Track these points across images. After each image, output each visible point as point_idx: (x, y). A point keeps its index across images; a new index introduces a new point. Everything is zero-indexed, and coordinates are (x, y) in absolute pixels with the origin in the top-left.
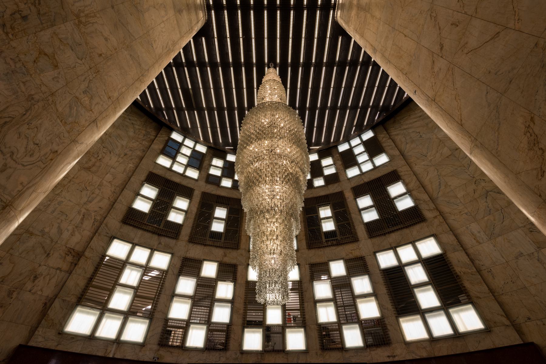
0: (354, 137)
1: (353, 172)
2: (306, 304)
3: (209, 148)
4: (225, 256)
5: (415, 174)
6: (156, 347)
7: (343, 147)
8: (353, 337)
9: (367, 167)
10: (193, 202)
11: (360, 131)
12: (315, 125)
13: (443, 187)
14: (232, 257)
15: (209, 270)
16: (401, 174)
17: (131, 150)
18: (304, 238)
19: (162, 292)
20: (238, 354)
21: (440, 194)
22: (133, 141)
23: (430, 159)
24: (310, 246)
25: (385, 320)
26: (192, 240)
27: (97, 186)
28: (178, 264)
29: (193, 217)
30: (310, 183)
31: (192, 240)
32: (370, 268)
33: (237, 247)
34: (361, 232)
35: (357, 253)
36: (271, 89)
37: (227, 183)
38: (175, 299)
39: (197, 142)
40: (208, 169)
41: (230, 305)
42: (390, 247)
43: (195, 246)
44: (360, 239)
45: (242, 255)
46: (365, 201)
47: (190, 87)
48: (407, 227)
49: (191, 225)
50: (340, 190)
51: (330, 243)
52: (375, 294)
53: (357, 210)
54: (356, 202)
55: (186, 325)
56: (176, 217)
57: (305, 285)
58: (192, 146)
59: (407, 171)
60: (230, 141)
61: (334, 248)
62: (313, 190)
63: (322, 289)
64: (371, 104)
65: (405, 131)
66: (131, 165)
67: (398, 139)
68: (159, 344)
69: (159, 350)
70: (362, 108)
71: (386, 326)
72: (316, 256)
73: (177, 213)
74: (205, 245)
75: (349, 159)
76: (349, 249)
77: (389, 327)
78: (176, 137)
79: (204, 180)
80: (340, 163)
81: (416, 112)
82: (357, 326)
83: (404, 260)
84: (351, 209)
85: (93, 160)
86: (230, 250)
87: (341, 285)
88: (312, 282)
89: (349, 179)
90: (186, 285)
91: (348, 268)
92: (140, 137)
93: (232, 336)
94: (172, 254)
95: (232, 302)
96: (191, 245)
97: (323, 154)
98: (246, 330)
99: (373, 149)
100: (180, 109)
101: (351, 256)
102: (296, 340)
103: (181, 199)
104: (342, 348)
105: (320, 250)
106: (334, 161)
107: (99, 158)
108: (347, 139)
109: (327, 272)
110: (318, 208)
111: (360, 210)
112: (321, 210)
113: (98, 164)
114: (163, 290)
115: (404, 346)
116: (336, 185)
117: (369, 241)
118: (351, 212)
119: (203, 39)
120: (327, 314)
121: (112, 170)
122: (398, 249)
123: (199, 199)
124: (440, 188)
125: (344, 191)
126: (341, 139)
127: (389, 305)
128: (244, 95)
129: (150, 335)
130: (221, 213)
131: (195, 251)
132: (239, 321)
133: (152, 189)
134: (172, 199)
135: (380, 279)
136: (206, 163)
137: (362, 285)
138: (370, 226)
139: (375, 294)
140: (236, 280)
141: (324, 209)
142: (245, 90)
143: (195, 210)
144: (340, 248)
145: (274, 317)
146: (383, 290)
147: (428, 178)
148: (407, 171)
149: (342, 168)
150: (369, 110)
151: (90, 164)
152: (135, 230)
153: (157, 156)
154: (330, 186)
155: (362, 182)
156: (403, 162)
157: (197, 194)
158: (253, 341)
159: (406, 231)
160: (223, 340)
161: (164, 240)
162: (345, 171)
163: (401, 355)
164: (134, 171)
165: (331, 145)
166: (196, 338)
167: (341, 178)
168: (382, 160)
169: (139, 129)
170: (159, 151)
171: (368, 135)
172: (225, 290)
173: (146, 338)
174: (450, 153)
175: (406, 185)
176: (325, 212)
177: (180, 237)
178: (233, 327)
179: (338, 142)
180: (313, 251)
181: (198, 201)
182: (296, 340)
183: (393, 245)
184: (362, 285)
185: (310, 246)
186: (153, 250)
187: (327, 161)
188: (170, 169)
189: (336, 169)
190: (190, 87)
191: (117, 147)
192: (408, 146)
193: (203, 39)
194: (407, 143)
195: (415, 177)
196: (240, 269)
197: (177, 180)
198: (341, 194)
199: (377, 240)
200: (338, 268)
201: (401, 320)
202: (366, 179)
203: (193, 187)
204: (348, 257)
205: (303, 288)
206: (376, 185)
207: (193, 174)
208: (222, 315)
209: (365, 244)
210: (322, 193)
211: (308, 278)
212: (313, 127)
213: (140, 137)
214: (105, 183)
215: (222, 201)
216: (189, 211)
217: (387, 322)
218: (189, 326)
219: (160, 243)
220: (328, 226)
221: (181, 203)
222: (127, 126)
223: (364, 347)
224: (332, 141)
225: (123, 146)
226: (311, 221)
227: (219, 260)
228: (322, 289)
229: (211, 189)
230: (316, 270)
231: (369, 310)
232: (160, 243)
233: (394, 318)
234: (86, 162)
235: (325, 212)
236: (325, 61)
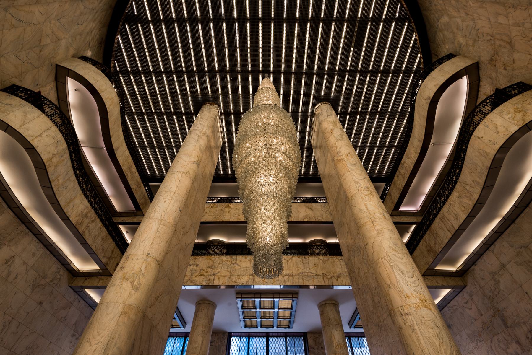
13: (14, 22)
21: (9, 16)
22: (449, 13)
23: (53, 22)
27: (521, 28)
36: (267, 93)
65: (95, 11)
66: (471, 4)
81: (98, 30)
85: (498, 43)
107: (492, 38)
113: (498, 37)
121: (492, 19)
124: (16, 19)
142: (295, 46)
147: (37, 13)
151: (503, 44)
174: (42, 44)
191: (468, 26)
192: (83, 7)
194: (85, 8)
213: (440, 9)
214: (511, 22)
225: (463, 21)
234: (505, 48)
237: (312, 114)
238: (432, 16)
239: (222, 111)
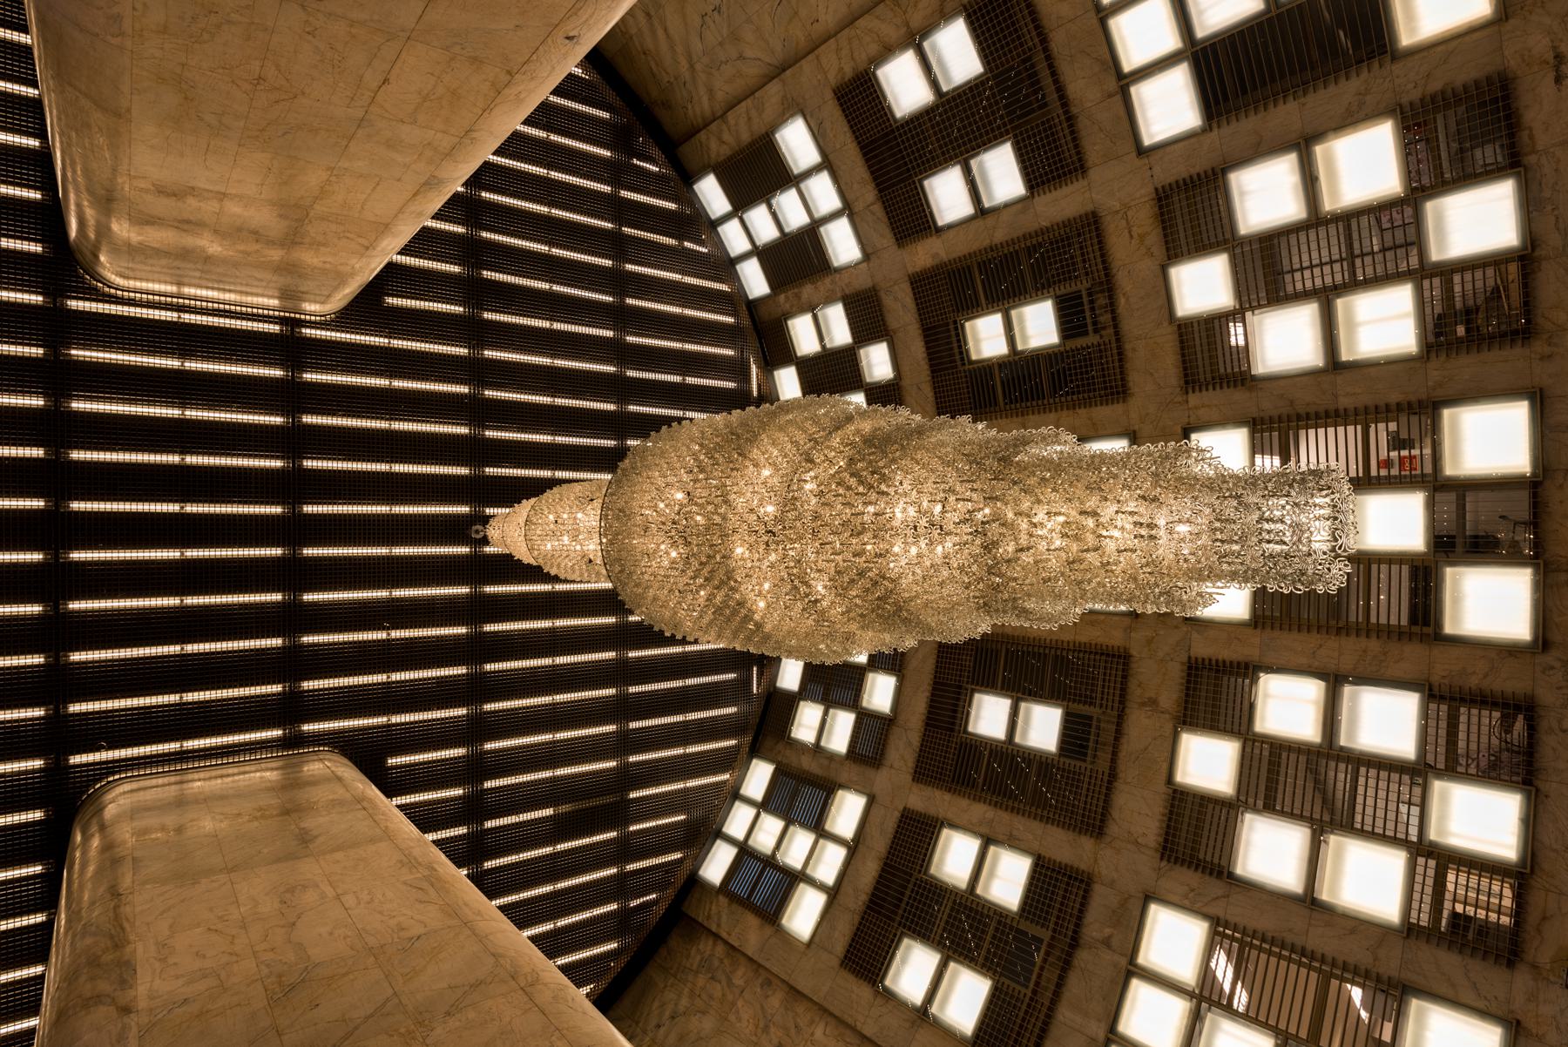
0: (719, 244)
1: (842, 244)
2: (1345, 402)
3: (755, 751)
4: (1153, 702)
5: (851, 21)
6: (1522, 979)
7: (754, 280)
8: (1478, 221)
9: (824, 193)
10: (950, 815)
11: (697, 223)
12: (677, 379)
14: (1158, 679)
15: (1208, 763)
16: (849, 72)
17: (766, 1029)
18: (1082, 412)
19: (1299, 941)
20: (1549, 658)
22: (732, 1018)
24: (1117, 390)
25: (1405, 100)
26: (1094, 822)
28: (1188, 877)
29: (1005, 816)
30: (882, 395)
31: (1094, 822)
32: (1200, 165)
33: (1120, 660)
34: (1064, 203)
35: (1144, 217)
36: (556, 532)
37: (880, 692)
38: (1324, 895)
40: (832, 756)
41: (1347, 690)
42: (1118, 98)
43: (1115, 813)
44: (1090, 208)
45: (1150, 641)
46: (947, 195)
47: (549, 812)
48: (1044, 40)
49: (1037, 826)
50: (906, 287)
51: (1105, 318)
52: (1303, 145)
53: (980, 223)
54: (950, 227)
55: (1433, 860)
56: (1008, 883)
57: (1268, 405)
58: (752, 812)
59: (838, 50)
60: (732, 676)
61: (1122, 301)
62: (906, 383)
63: (1284, 341)
64: (607, 189)
65: (698, 67)
66: (819, 1033)
67: (724, 89)
68: (1511, 964)
69: (1535, 967)
70: (619, 220)
71: (1433, 97)
72: (1152, 367)
73: (992, 874)
74: (1113, 775)
75: (796, 259)
76: (1128, 249)
77: (1436, 86)
78: (717, 865)
79: (870, 772)
80: (807, 291)
81: (633, 31)
82: (1430, 207)
83: (1170, 41)
84: (976, 246)
86: (1133, 684)
87: (1267, 270)
88: (1254, 378)
89: (867, 256)
90: (1270, 851)
91: (1201, 248)
92: (718, 993)
93: (1473, 682)
94: (1148, 898)
95: (1335, 681)
96: (1113, 829)
97: (778, 351)
98: (1448, 629)
99: (758, 175)
100: (624, 850)
101: (1154, 238)
102: (1491, 439)
103: (942, 860)
104: (1523, 261)
105: (1129, 354)
106: (802, 310)
108: (726, 266)
109: (1214, 323)
110: (971, 362)
111: (981, 211)
112: (978, 351)
114: (1289, 938)
115: (1511, 21)
116: (887, 301)
117: (1093, 174)
118: (987, 243)
119: (392, 761)
120: (1384, 323)
122: (1128, 66)
123: (938, 793)
125: (911, 270)
126: (725, 288)
127: (1348, 89)
128: (576, 628)
129: (1469, 997)
130: (989, 716)
131: (1138, 814)
132: (1413, 656)
133: (904, 961)
134: (941, 890)
135: (1244, 127)
136: (808, 764)
137: (1265, 195)
138: (1036, 175)
139: (1303, 145)
140: (1247, 666)
141: (977, 341)
143: (980, 811)
144: (1123, 280)
145: (1395, 523)
146: (1286, 114)
148: (838, 50)
149: (827, 281)
150: (624, 193)
152: (1055, 1031)
153: (787, 938)
154: (892, 323)
155: (878, 209)
156: (807, 66)
157: (922, 799)
158: (1492, 603)
159: (1058, 41)
160: (1516, 718)
161: (1095, 925)
162: (838, 270)
164: (840, 1021)
165: (746, 322)
166: (1482, 819)
167: (862, 282)
168: (797, 142)
169: (692, 994)
170: (769, 930)
171: (712, 194)
172: (1288, 706)
173: (1484, 1014)
175: (887, 52)
176: (986, 337)
177: (1083, 867)
178: (1435, 679)
179: (736, 300)
180: (1135, 379)
181: (947, 796)
182: (1491, 439)
183: (1112, 84)
184: (1265, 195)
185: (1117, 390)
186: (1132, 970)
187: (803, 336)
188: (833, 893)
189: (829, 301)
190: (549, 812)
192: (749, 53)
193: (392, 761)
194: (741, 57)
195: (861, 23)
196: (1202, 649)
197: (869, 870)
198: (922, 284)
199: (1094, 148)
200: (1202, 285)
201: (1406, 40)
202: (867, 194)
203: (897, 814)
204: (1159, 252)
205: (1279, 413)
206: (889, 159)
207: (847, 811)
208: (1387, 721)
209: (1109, 190)
210: (917, 348)
211: (1238, 395)
212: (683, 386)
213: (718, 993)
215: (947, 710)
216: (984, 830)
217: (1415, 95)
218: (1433, 845)
219: (1107, 942)
220: (1039, 325)
221: (955, 857)
222: (681, 1038)
223: (1518, 176)
224: (730, 320)
226: (1021, 388)
227: (1169, 727)
228: (1284, 341)
229: (903, 750)
230: (1208, 369)
231: (1365, 164)
232: (1107, 942)
233: (1397, 68)
235: (986, 337)
236: (463, 351)
237: (295, 742)
238: (670, 995)
239: (307, 331)
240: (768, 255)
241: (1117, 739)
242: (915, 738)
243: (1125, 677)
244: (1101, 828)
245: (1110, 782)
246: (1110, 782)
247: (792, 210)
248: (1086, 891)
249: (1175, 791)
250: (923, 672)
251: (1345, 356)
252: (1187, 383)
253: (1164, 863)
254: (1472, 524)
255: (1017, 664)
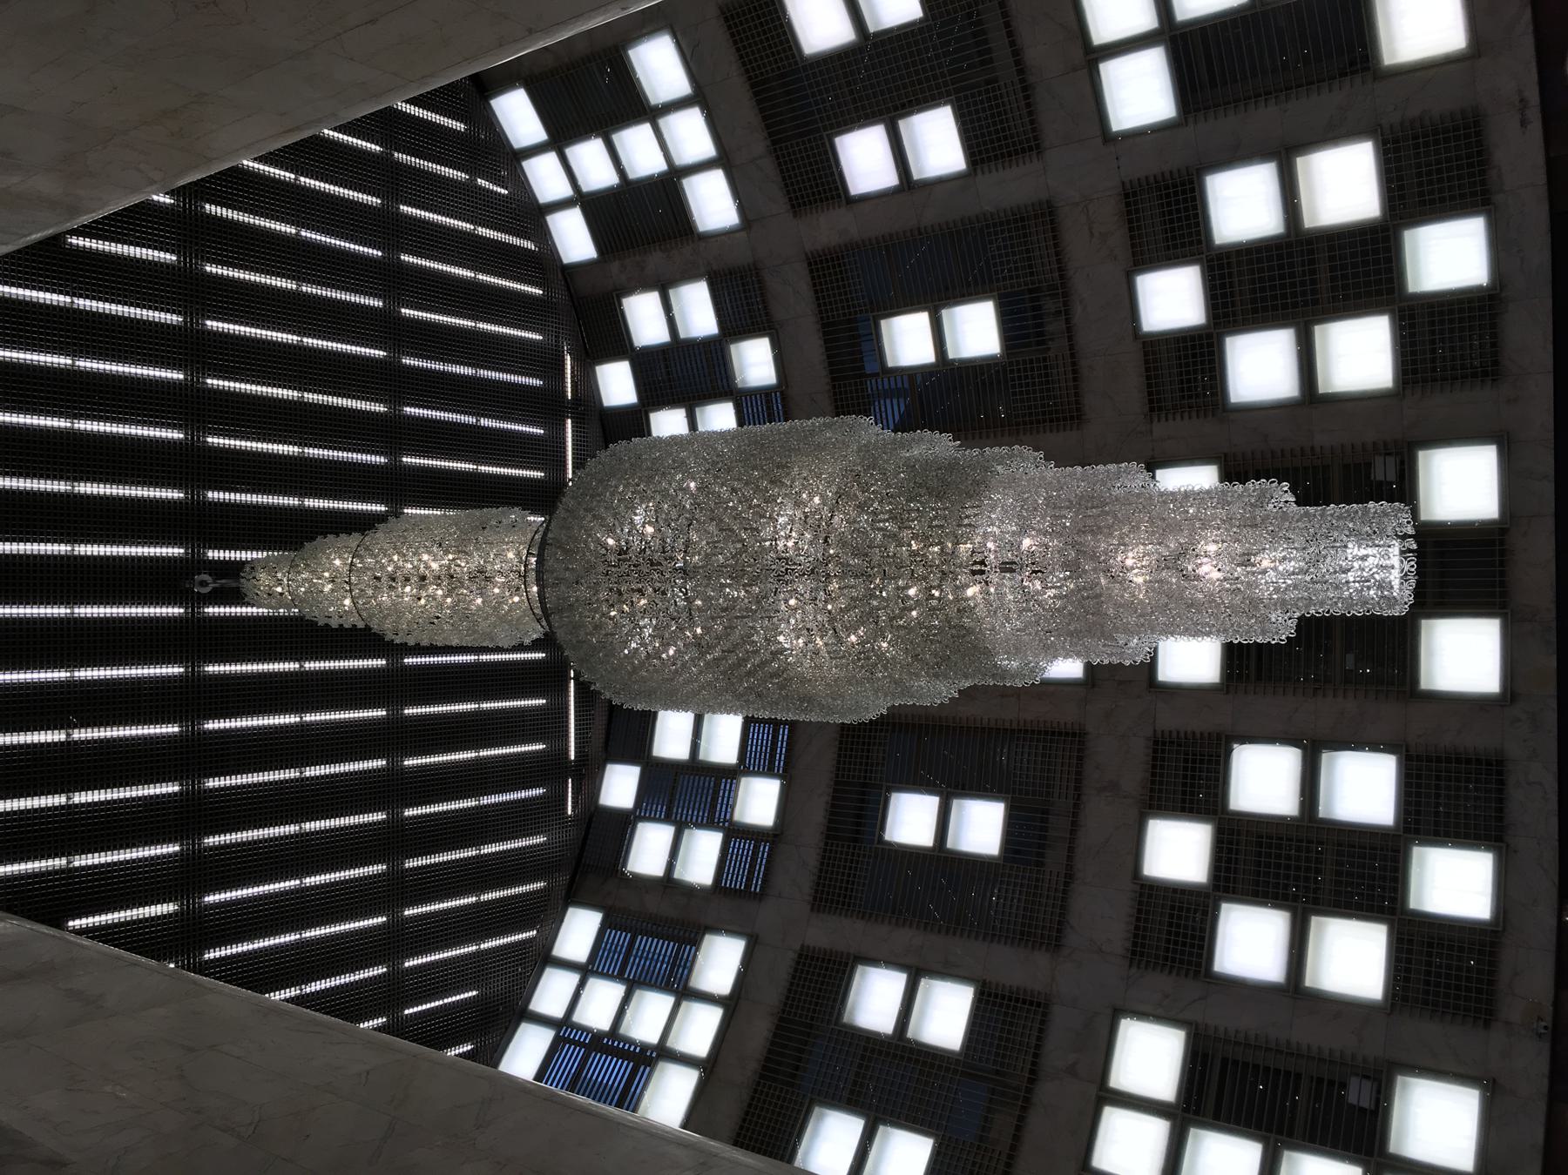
0: (521, 184)
1: (713, 204)
3: (575, 896)
7: (573, 239)
8: (1450, 256)
9: (691, 135)
14: (1119, 757)
15: (1177, 851)
28: (1159, 982)
30: (751, 404)
33: (1073, 740)
34: (1015, 186)
37: (759, 802)
39: (541, 957)
40: (689, 891)
46: (864, 159)
54: (865, 198)
58: (573, 979)
68: (1487, 1024)
72: (1115, 392)
74: (1069, 877)
75: (643, 223)
80: (655, 260)
90: (1250, 942)
97: (612, 339)
98: (1424, 684)
106: (645, 286)
108: (531, 215)
120: (1360, 354)
130: (911, 819)
131: (1100, 920)
137: (1242, 205)
143: (906, 937)
145: (1375, 567)
146: (1266, 118)
155: (768, 165)
157: (824, 933)
158: (1464, 656)
161: (1056, 1053)
163: (1518, 74)
168: (659, 65)
172: (1263, 779)
176: (908, 340)
179: (544, 263)
182: (1462, 483)
184: (1242, 205)
187: (645, 318)
196: (1169, 721)
197: (759, 1031)
202: (757, 145)
203: (792, 955)
210: (813, 348)
220: (976, 330)
235: (908, 340)
240: (599, 209)
241: (1073, 832)
242: (812, 858)
243: (1080, 758)
244: (1058, 939)
245: (1066, 884)
246: (1066, 884)
247: (641, 151)
248: (1045, 1014)
249: (1142, 886)
250: (821, 763)
251: (1322, 389)
252: (1152, 410)
253: (1134, 970)
254: (1456, 568)
255: (947, 753)
